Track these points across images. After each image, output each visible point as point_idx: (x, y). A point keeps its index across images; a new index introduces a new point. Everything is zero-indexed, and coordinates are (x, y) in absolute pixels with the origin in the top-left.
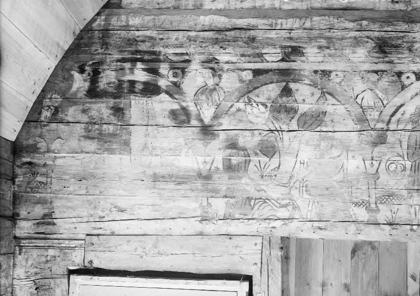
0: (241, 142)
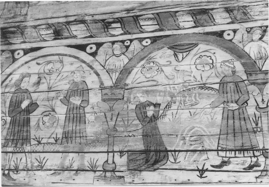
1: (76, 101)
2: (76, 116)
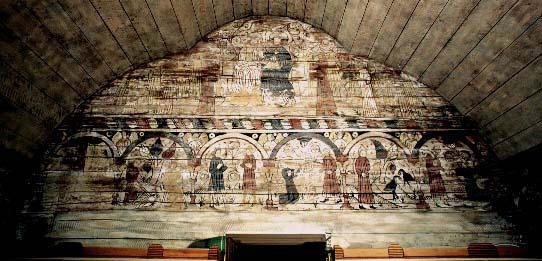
0: (135, 165)
1: (249, 166)
2: (249, 173)
